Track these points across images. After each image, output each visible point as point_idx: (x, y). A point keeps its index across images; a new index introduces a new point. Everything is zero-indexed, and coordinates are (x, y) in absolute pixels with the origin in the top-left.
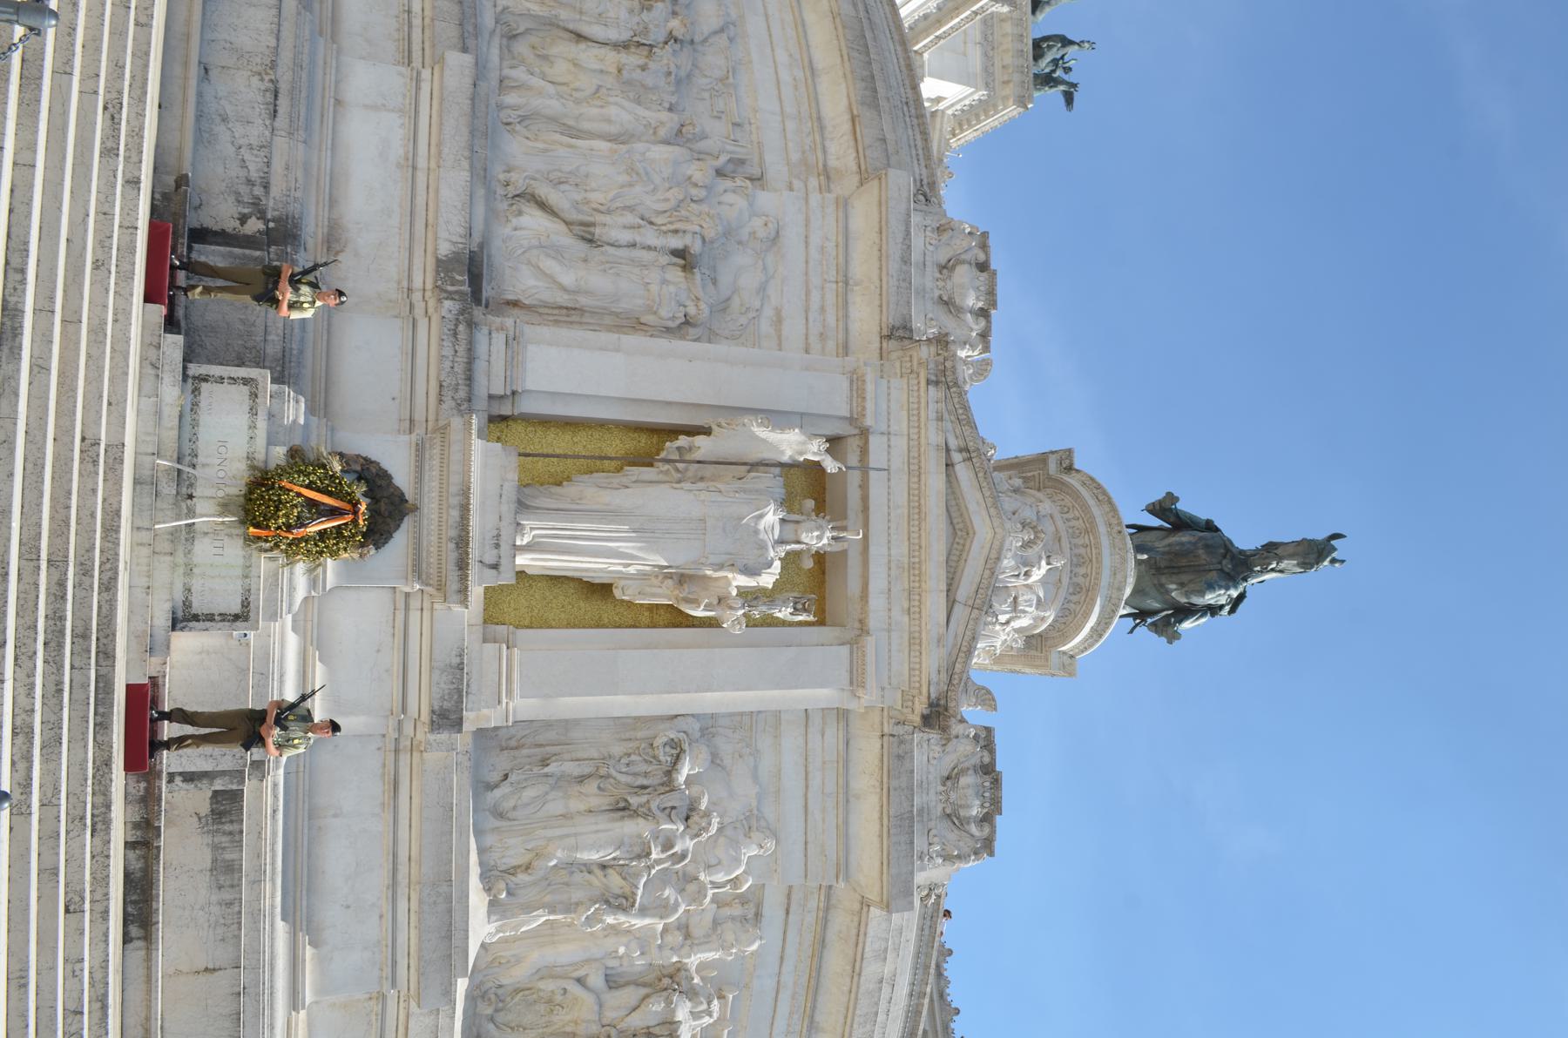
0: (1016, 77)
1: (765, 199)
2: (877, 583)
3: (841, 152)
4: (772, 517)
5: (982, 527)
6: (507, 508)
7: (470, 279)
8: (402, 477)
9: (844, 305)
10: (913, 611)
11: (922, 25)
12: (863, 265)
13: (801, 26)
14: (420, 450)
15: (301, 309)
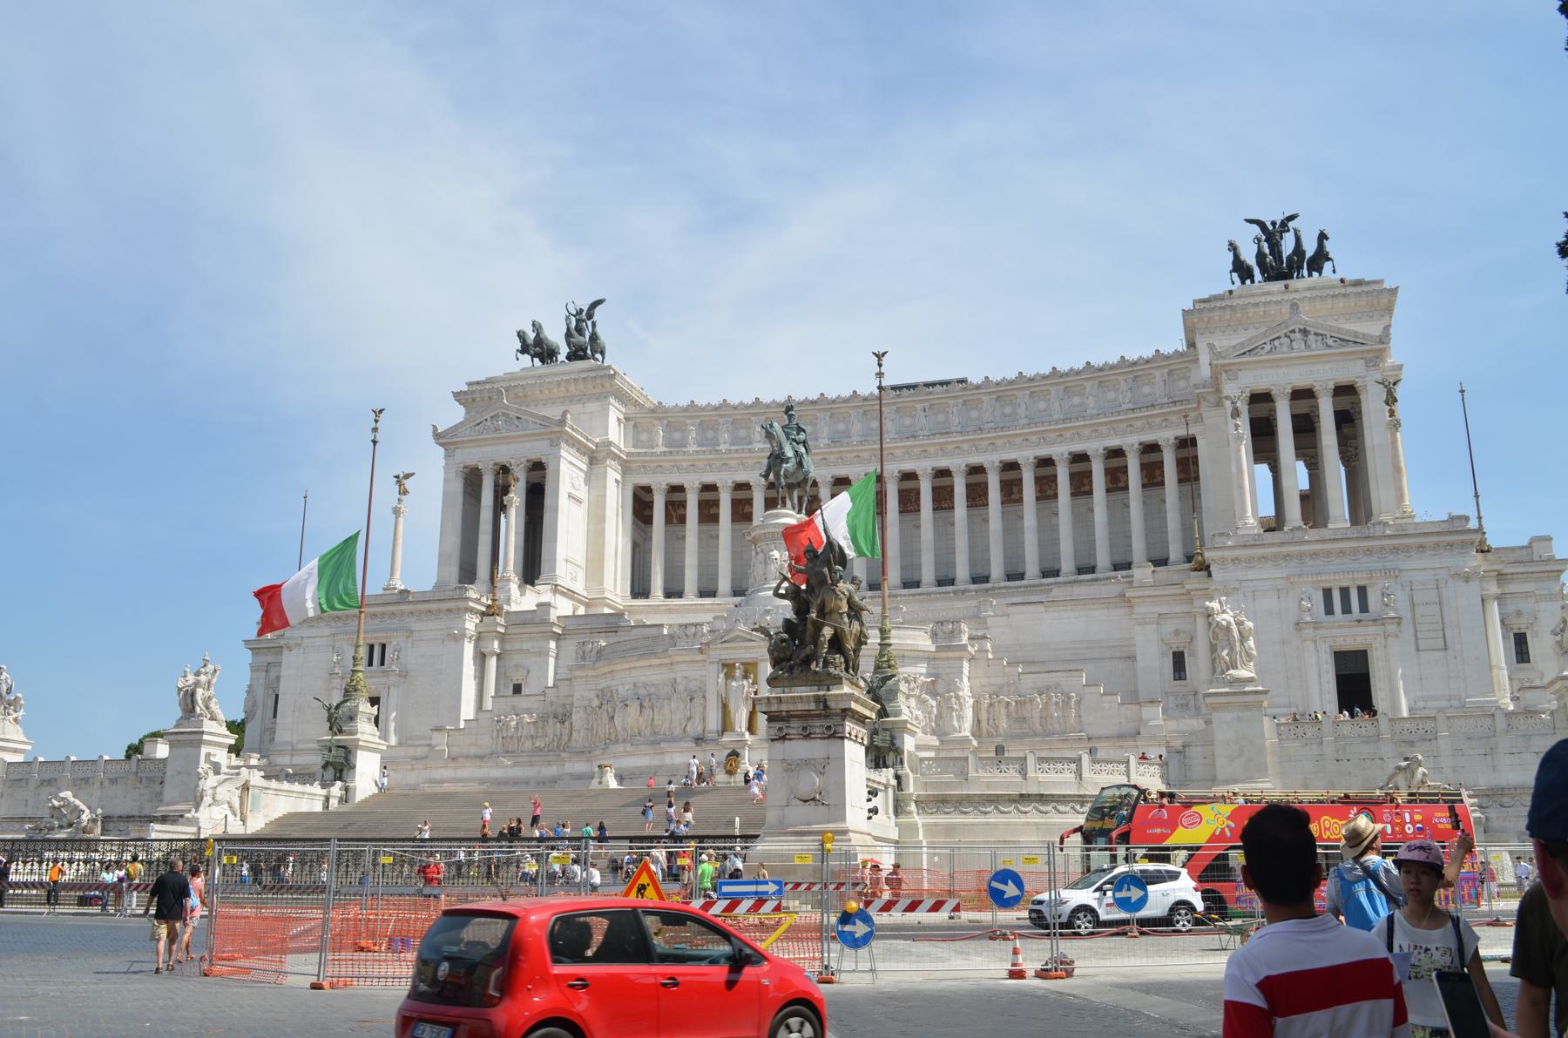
0: (599, 381)
3: (667, 661)
7: (699, 740)
12: (688, 658)
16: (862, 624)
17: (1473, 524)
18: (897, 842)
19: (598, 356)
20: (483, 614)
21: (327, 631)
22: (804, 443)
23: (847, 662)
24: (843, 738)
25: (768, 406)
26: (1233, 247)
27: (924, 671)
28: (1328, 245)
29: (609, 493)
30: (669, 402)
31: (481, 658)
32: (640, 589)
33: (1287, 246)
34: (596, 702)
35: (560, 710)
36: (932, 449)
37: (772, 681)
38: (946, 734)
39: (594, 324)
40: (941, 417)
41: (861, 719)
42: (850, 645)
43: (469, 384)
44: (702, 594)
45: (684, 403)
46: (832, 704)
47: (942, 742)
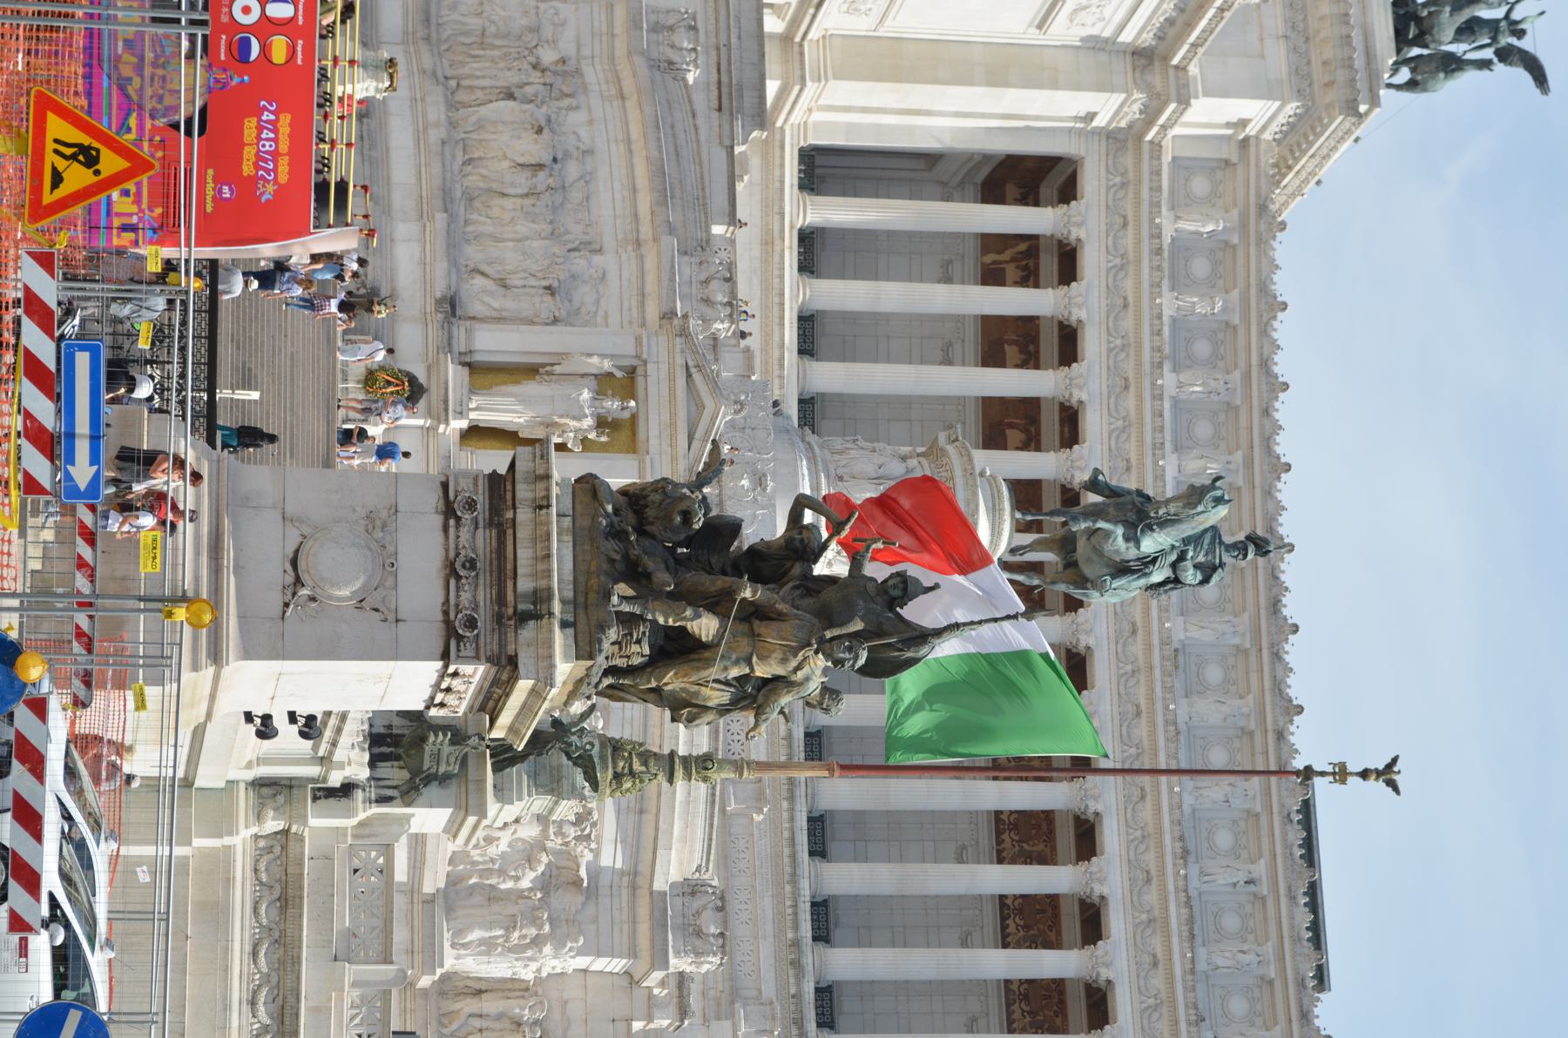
0: (1341, 75)
1: (597, 259)
2: (654, 432)
3: (646, 231)
4: (586, 395)
5: (709, 404)
6: (465, 391)
7: (451, 306)
8: (422, 379)
9: (642, 304)
10: (673, 445)
11: (1172, 32)
12: (651, 286)
13: (631, 168)
14: (429, 368)
15: (382, 313)
16: (723, 710)
18: (188, 783)
19: (1404, 75)
22: (1175, 581)
23: (631, 671)
24: (445, 656)
25: (1269, 493)
27: (606, 861)
29: (1062, 95)
30: (1283, 248)
32: (824, 169)
34: (548, 56)
36: (1152, 897)
37: (589, 486)
38: (449, 910)
39: (1485, 64)
40: (1231, 922)
41: (490, 703)
42: (673, 681)
44: (807, 322)
45: (1283, 285)
46: (528, 632)
47: (430, 900)
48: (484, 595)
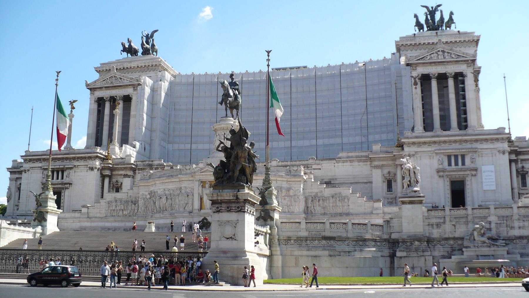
17: (507, 131)
19: (155, 53)
20: (104, 159)
21: (40, 165)
23: (247, 179)
24: (244, 212)
26: (416, 16)
28: (453, 17)
31: (103, 177)
33: (437, 17)
34: (148, 197)
35: (134, 200)
39: (153, 40)
41: (253, 204)
42: (248, 171)
43: (101, 64)
46: (240, 197)
48: (233, 205)
